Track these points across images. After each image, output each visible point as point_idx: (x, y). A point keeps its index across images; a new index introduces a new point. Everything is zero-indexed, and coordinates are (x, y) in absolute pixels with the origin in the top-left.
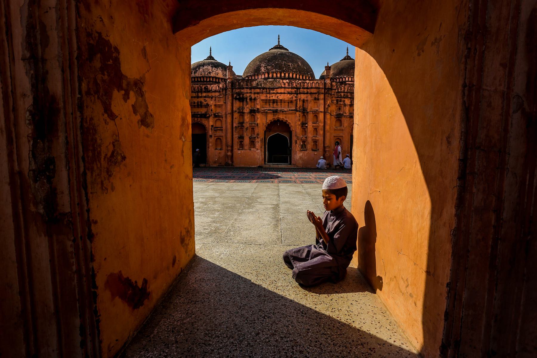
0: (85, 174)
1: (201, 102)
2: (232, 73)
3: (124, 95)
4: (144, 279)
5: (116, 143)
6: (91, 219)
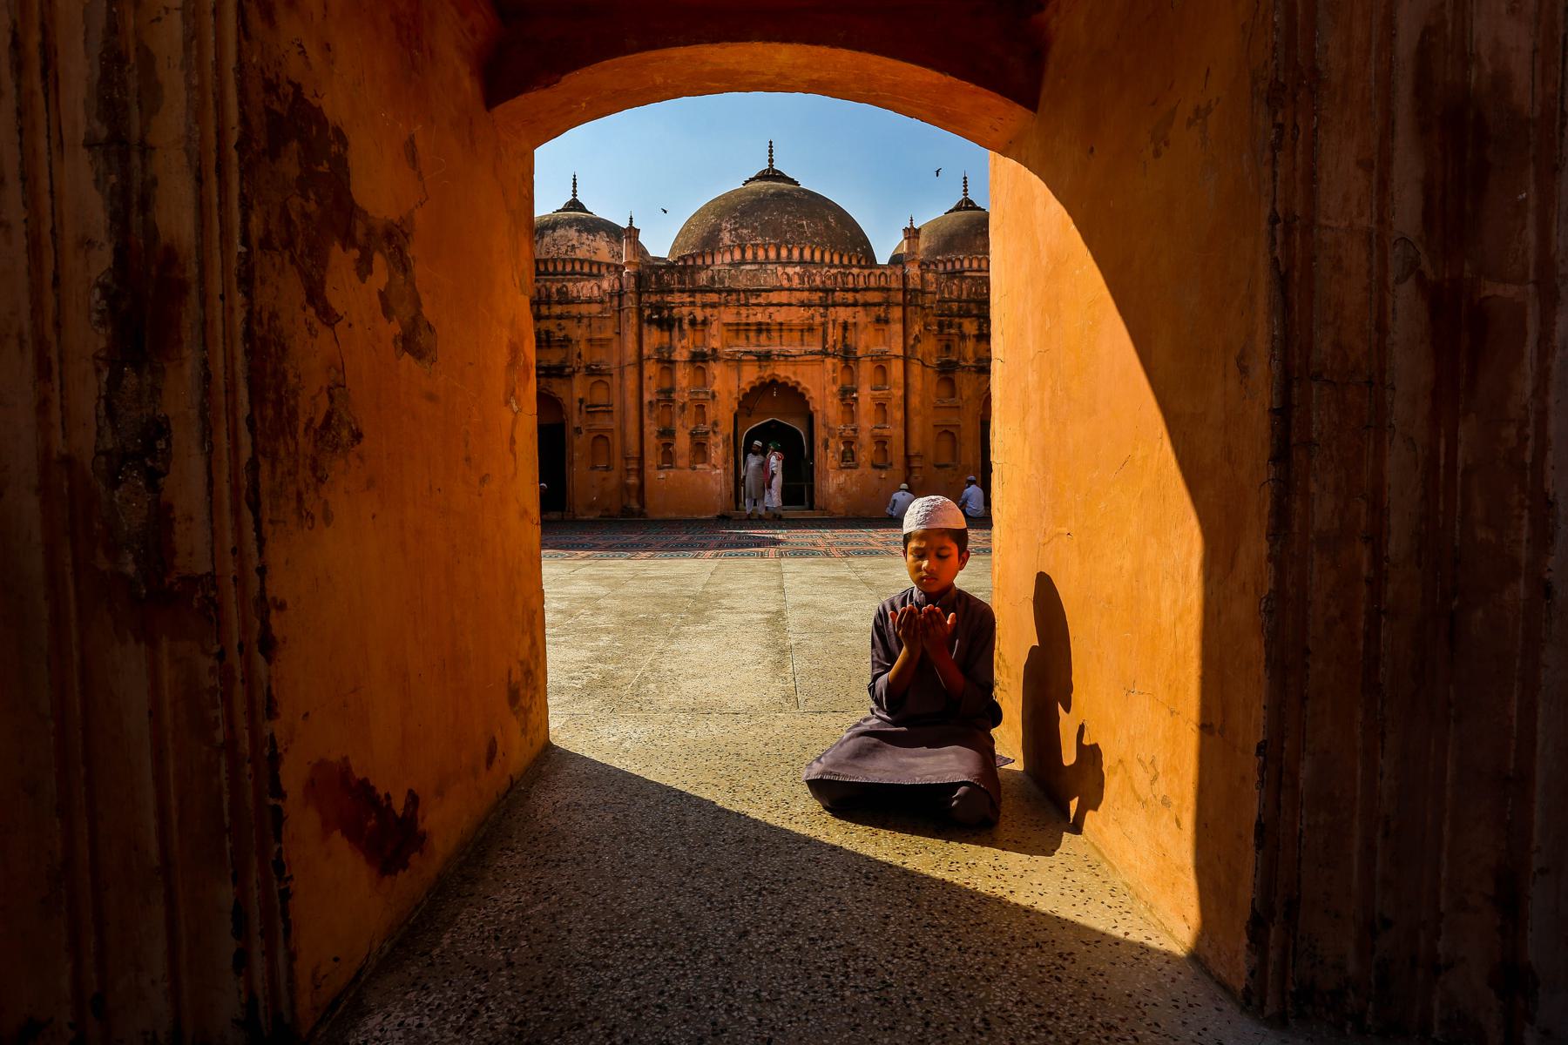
0: (254, 465)
1: (548, 332)
2: (640, 250)
3: (360, 260)
4: (410, 791)
5: (335, 390)
6: (269, 596)
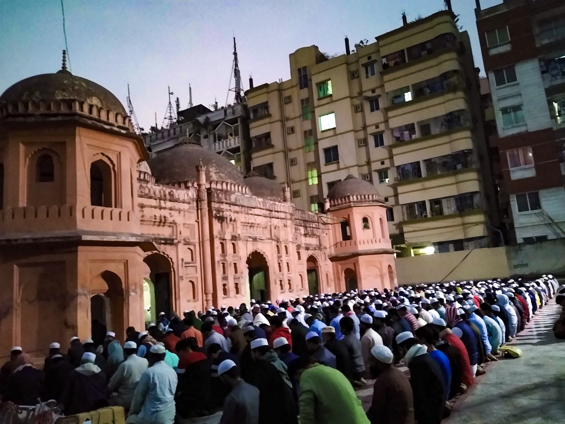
1: (165, 217)
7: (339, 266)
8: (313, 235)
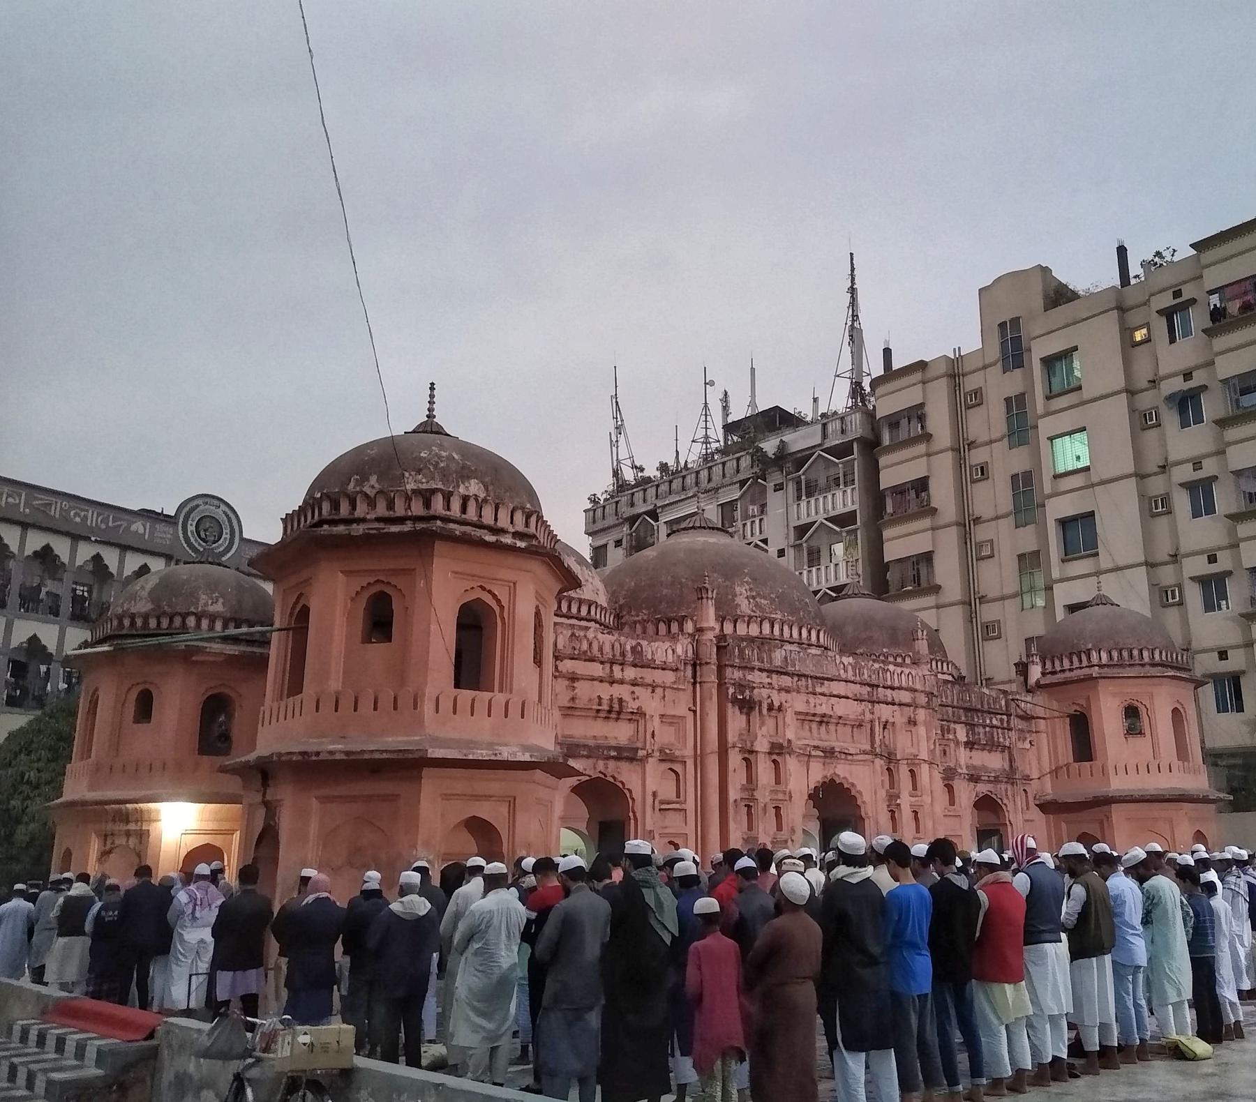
1: (620, 700)
7: (1064, 826)
8: (992, 746)
